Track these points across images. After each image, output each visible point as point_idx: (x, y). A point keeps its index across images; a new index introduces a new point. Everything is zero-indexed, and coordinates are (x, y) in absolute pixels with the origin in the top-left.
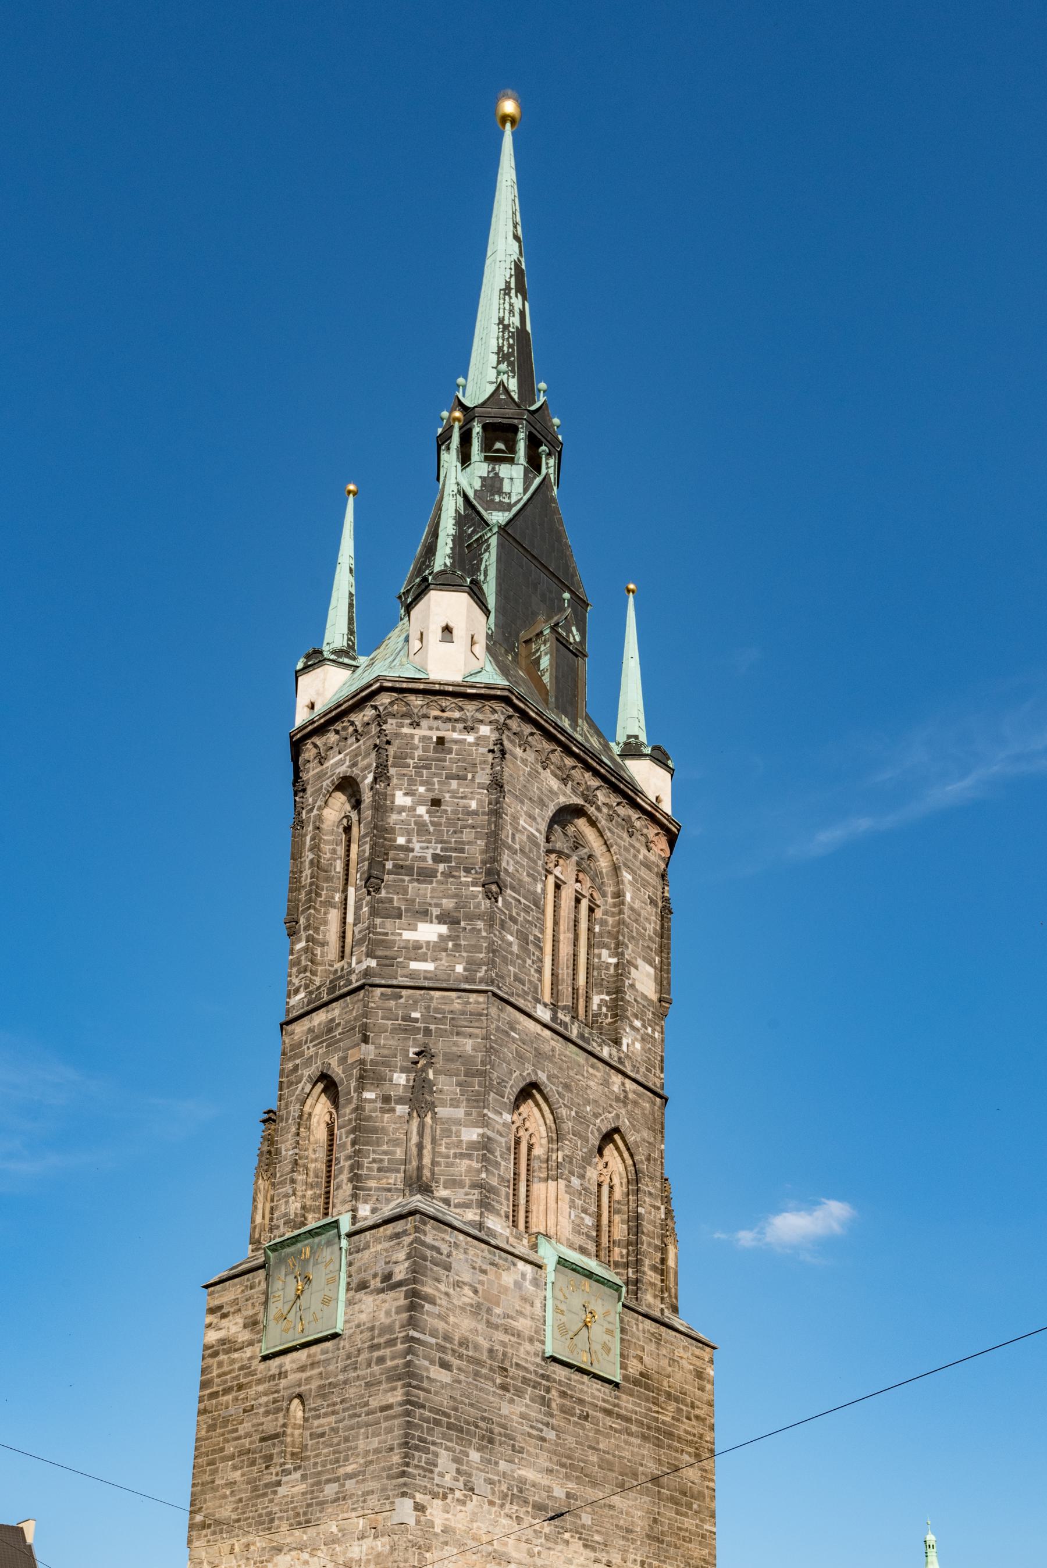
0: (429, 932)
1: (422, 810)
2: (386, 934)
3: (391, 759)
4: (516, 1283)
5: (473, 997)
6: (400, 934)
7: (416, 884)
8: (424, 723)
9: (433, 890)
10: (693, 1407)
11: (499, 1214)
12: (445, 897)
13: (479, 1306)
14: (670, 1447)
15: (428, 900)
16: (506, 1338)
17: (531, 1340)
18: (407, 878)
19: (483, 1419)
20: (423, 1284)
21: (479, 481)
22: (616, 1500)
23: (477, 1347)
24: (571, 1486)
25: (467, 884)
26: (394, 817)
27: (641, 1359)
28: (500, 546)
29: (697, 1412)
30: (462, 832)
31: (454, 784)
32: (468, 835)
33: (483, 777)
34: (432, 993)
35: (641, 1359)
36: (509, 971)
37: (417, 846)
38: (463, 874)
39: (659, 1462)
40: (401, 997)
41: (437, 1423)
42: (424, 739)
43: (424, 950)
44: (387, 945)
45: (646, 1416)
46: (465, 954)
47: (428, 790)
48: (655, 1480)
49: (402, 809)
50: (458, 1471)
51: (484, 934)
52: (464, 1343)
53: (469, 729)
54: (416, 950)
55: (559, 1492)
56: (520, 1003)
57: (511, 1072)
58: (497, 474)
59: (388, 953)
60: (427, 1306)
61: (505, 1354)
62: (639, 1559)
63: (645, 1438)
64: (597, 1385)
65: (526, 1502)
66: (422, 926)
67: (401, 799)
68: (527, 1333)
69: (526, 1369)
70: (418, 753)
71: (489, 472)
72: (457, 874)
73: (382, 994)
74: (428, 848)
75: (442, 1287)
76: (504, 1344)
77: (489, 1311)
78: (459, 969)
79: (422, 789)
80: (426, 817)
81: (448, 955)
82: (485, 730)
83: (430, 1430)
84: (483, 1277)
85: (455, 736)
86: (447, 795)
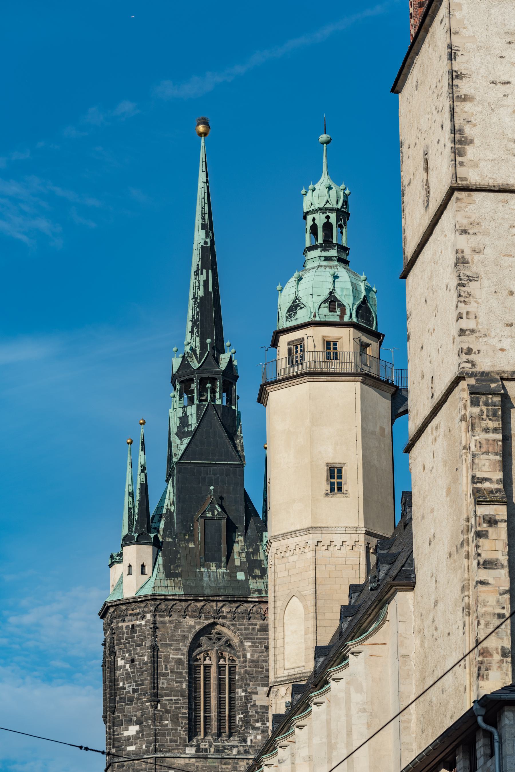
0: (133, 730)
1: (127, 666)
2: (118, 735)
3: (115, 642)
5: (149, 761)
6: (123, 734)
7: (127, 706)
8: (127, 619)
9: (133, 708)
12: (138, 710)
15: (132, 714)
18: (124, 704)
21: (178, 420)
25: (144, 702)
26: (118, 672)
28: (179, 472)
30: (142, 674)
31: (138, 648)
32: (144, 676)
33: (148, 644)
34: (135, 761)
36: (167, 739)
37: (126, 686)
38: (143, 697)
40: (124, 766)
42: (127, 627)
43: (131, 740)
44: (118, 740)
46: (145, 739)
47: (129, 655)
49: (121, 667)
51: (152, 727)
53: (143, 618)
54: (129, 741)
56: (176, 753)
58: (186, 414)
59: (119, 744)
66: (130, 728)
67: (121, 662)
70: (125, 635)
71: (183, 413)
72: (141, 697)
73: (118, 766)
74: (130, 686)
78: (144, 747)
79: (127, 655)
80: (129, 670)
81: (140, 741)
82: (149, 616)
85: (138, 622)
86: (136, 656)
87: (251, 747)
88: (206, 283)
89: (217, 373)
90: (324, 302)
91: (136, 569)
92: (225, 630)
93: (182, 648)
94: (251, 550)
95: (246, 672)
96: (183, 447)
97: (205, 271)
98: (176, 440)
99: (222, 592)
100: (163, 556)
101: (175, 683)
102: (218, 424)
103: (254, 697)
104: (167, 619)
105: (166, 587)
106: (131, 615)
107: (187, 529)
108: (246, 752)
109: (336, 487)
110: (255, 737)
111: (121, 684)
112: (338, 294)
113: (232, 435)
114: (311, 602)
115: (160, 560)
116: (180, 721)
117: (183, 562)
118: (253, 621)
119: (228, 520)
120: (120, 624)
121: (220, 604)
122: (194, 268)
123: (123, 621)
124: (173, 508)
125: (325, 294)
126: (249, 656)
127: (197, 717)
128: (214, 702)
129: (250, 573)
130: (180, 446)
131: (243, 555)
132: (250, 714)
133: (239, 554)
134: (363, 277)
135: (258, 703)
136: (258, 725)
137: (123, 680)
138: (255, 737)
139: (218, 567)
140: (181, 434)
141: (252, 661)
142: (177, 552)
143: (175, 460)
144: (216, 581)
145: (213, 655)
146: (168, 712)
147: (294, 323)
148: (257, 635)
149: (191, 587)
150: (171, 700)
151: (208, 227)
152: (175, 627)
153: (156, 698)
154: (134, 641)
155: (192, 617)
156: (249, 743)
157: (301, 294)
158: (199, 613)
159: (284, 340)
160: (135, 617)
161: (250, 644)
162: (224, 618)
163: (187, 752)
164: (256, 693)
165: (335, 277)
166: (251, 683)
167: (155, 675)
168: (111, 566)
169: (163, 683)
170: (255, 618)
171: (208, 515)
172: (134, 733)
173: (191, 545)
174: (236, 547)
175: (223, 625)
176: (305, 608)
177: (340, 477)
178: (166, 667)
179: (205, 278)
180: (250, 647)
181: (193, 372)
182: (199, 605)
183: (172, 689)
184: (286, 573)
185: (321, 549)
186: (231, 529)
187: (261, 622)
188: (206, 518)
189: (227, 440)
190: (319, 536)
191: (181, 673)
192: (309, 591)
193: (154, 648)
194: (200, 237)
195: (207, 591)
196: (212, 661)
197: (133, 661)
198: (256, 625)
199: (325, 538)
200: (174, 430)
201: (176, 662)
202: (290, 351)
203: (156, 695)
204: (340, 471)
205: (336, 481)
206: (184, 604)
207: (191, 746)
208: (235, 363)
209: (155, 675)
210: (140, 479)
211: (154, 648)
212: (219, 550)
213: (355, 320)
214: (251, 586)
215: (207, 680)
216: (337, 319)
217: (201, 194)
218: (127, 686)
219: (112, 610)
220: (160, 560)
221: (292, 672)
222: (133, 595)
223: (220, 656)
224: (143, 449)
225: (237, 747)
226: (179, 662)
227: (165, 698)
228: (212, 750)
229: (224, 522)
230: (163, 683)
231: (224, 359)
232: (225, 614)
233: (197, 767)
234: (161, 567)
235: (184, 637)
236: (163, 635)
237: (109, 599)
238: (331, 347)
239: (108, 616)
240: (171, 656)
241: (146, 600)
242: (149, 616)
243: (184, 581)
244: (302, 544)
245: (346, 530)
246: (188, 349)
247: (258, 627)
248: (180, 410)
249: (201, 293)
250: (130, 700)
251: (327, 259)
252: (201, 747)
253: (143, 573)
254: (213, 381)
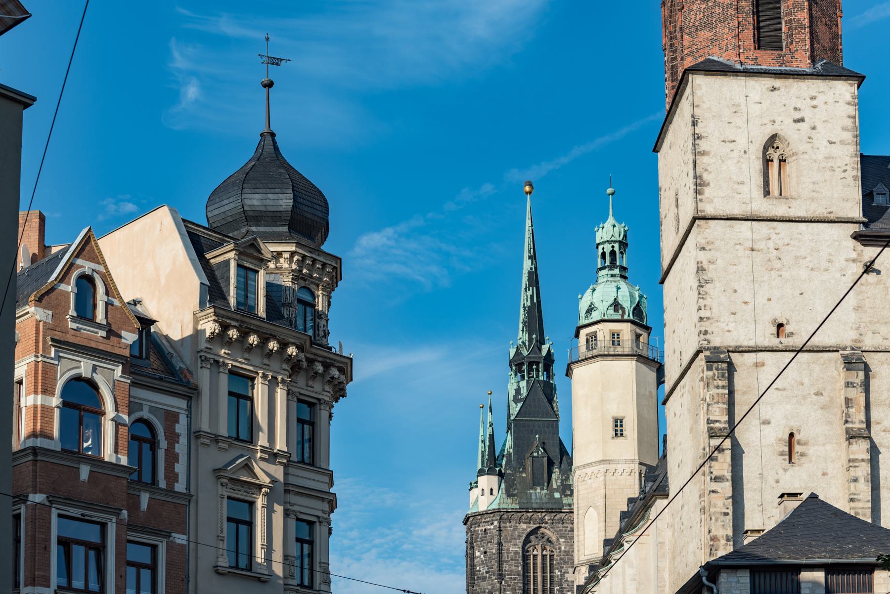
26: (476, 560)
28: (515, 426)
33: (496, 541)
67: (477, 554)
82: (496, 523)
88: (532, 296)
89: (540, 358)
90: (611, 306)
91: (487, 492)
92: (547, 531)
95: (561, 559)
96: (518, 409)
98: (512, 404)
99: (545, 506)
100: (505, 482)
101: (513, 567)
102: (541, 393)
103: (566, 575)
104: (508, 524)
107: (521, 464)
109: (619, 433)
112: (620, 300)
113: (550, 401)
114: (602, 511)
115: (503, 486)
117: (519, 487)
118: (565, 525)
119: (549, 458)
121: (543, 514)
122: (524, 286)
124: (511, 451)
125: (611, 301)
126: (563, 548)
127: (529, 589)
128: (539, 579)
129: (563, 493)
130: (515, 408)
134: (637, 288)
139: (542, 489)
140: (516, 400)
141: (565, 551)
142: (514, 480)
143: (512, 418)
144: (541, 498)
145: (539, 548)
146: (509, 586)
147: (590, 321)
151: (533, 258)
153: (501, 577)
155: (525, 523)
157: (594, 301)
158: (529, 520)
159: (583, 333)
162: (546, 523)
165: (618, 288)
167: (500, 562)
168: (470, 490)
173: (524, 475)
174: (554, 476)
175: (545, 528)
176: (599, 514)
177: (621, 426)
181: (524, 358)
182: (529, 515)
183: (512, 571)
184: (585, 492)
185: (609, 474)
186: (551, 463)
188: (534, 457)
189: (547, 404)
190: (607, 466)
192: (601, 503)
193: (500, 544)
194: (527, 264)
195: (535, 506)
196: (538, 552)
197: (485, 553)
199: (612, 467)
200: (511, 398)
202: (587, 340)
203: (501, 575)
204: (621, 422)
205: (619, 428)
206: (520, 514)
208: (552, 351)
209: (500, 562)
210: (489, 431)
211: (500, 544)
212: (543, 478)
213: (631, 317)
215: (535, 564)
216: (620, 317)
217: (528, 235)
218: (482, 569)
219: (471, 519)
220: (503, 486)
221: (589, 557)
222: (485, 509)
223: (544, 549)
224: (491, 411)
226: (516, 553)
229: (545, 459)
230: (506, 567)
231: (545, 349)
235: (520, 536)
237: (469, 512)
238: (615, 337)
239: (469, 523)
241: (494, 512)
242: (496, 523)
244: (596, 472)
245: (626, 462)
246: (520, 342)
248: (515, 384)
249: (529, 304)
250: (484, 579)
251: (612, 276)
253: (491, 494)
254: (537, 364)
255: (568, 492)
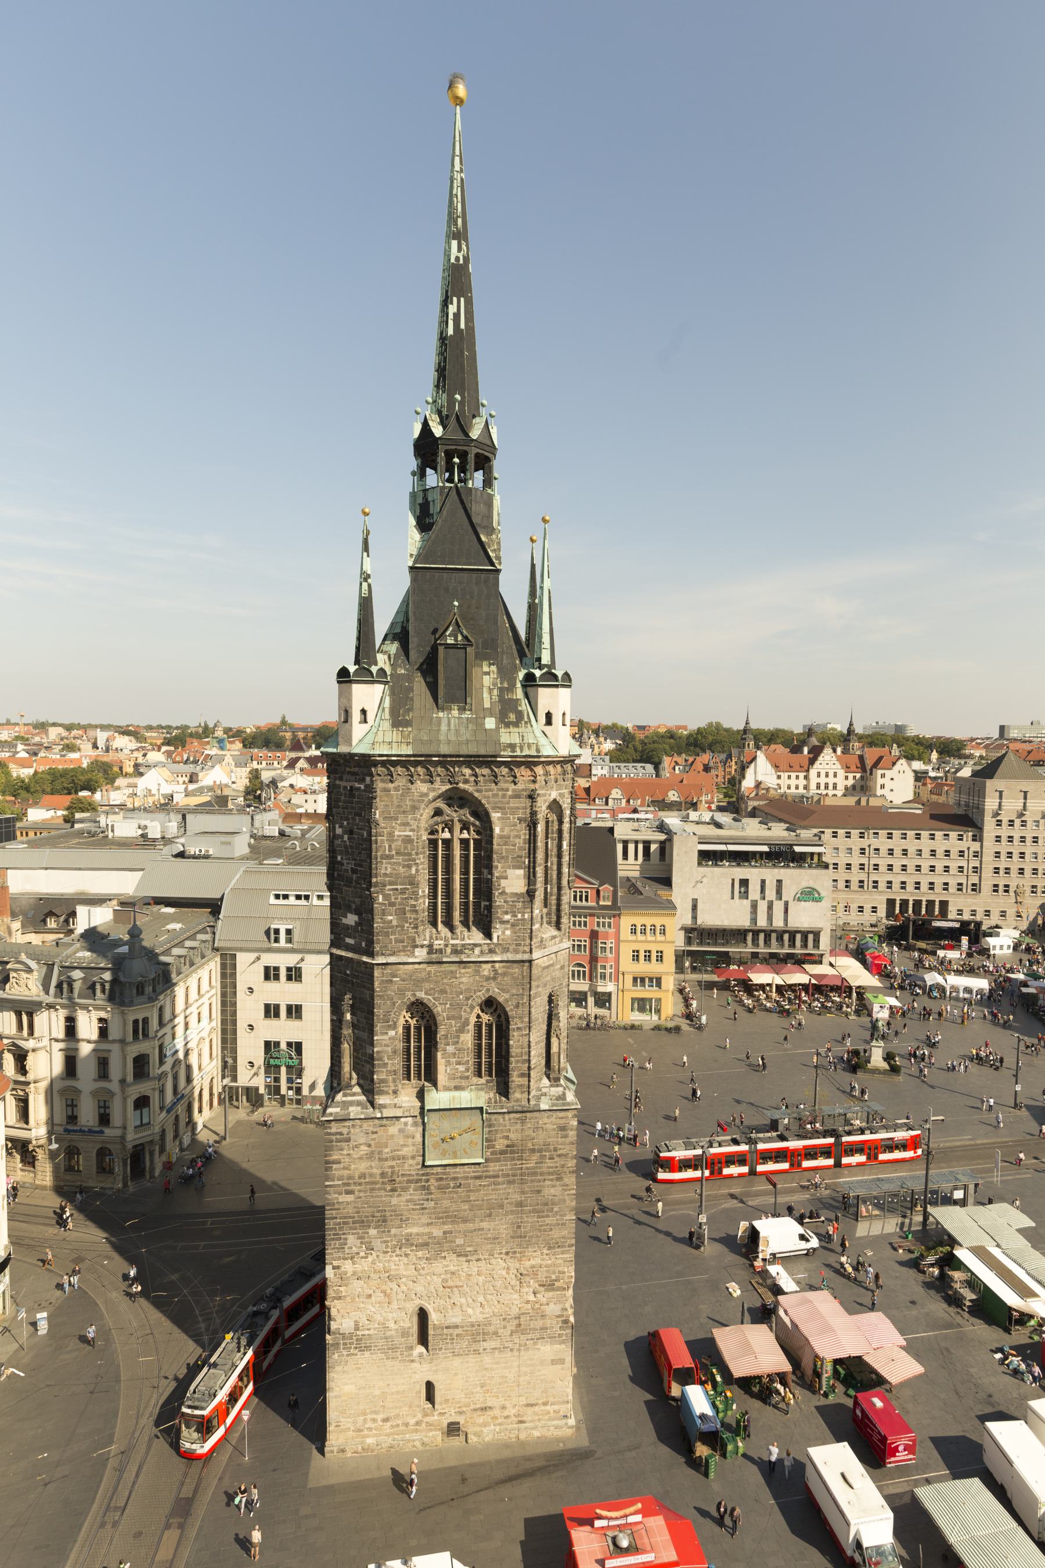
1: (346, 837)
4: (400, 1130)
8: (345, 777)
10: (555, 1150)
11: (387, 1093)
13: (372, 1153)
14: (532, 1181)
16: (394, 1163)
17: (413, 1157)
19: (378, 1211)
20: (331, 1155)
22: (485, 1225)
23: (371, 1175)
24: (447, 1227)
27: (507, 1138)
29: (559, 1152)
35: (507, 1138)
37: (345, 862)
39: (523, 1193)
41: (345, 1223)
45: (511, 1169)
48: (520, 1204)
50: (362, 1243)
52: (363, 1176)
55: (437, 1232)
57: (394, 1004)
60: (334, 1166)
61: (392, 1172)
62: (504, 1251)
63: (509, 1182)
64: (466, 1168)
65: (412, 1245)
66: (349, 915)
68: (410, 1155)
69: (410, 1175)
75: (345, 1152)
76: (392, 1167)
77: (380, 1153)
83: (341, 1229)
84: (375, 1136)
85: (357, 785)
87: (498, 945)
88: (457, 316)
93: (412, 822)
94: (506, 685)
97: (455, 299)
103: (503, 883)
105: (390, 743)
106: (349, 773)
108: (491, 951)
110: (503, 933)
111: (339, 858)
116: (408, 915)
120: (338, 782)
123: (341, 779)
126: (497, 830)
131: (495, 692)
132: (498, 903)
133: (490, 690)
135: (507, 891)
136: (507, 917)
137: (341, 854)
138: (503, 933)
139: (462, 710)
141: (501, 837)
146: (392, 904)
148: (508, 803)
149: (422, 742)
150: (397, 889)
152: (402, 795)
154: (353, 808)
155: (423, 781)
156: (495, 940)
160: (353, 778)
161: (499, 815)
162: (466, 782)
163: (417, 954)
164: (506, 878)
166: (499, 865)
169: (386, 869)
170: (506, 781)
171: (449, 641)
172: (353, 924)
178: (390, 846)
179: (455, 310)
180: (499, 819)
183: (398, 876)
187: (512, 786)
188: (448, 646)
191: (410, 854)
195: (444, 750)
198: (507, 790)
201: (403, 841)
207: (422, 946)
214: (502, 740)
225: (480, 945)
226: (408, 840)
227: (388, 887)
228: (449, 950)
232: (467, 777)
233: (429, 973)
234: (387, 711)
236: (386, 805)
240: (397, 833)
243: (416, 732)
247: (510, 793)
249: (450, 331)
252: (435, 947)
255: (512, 717)
